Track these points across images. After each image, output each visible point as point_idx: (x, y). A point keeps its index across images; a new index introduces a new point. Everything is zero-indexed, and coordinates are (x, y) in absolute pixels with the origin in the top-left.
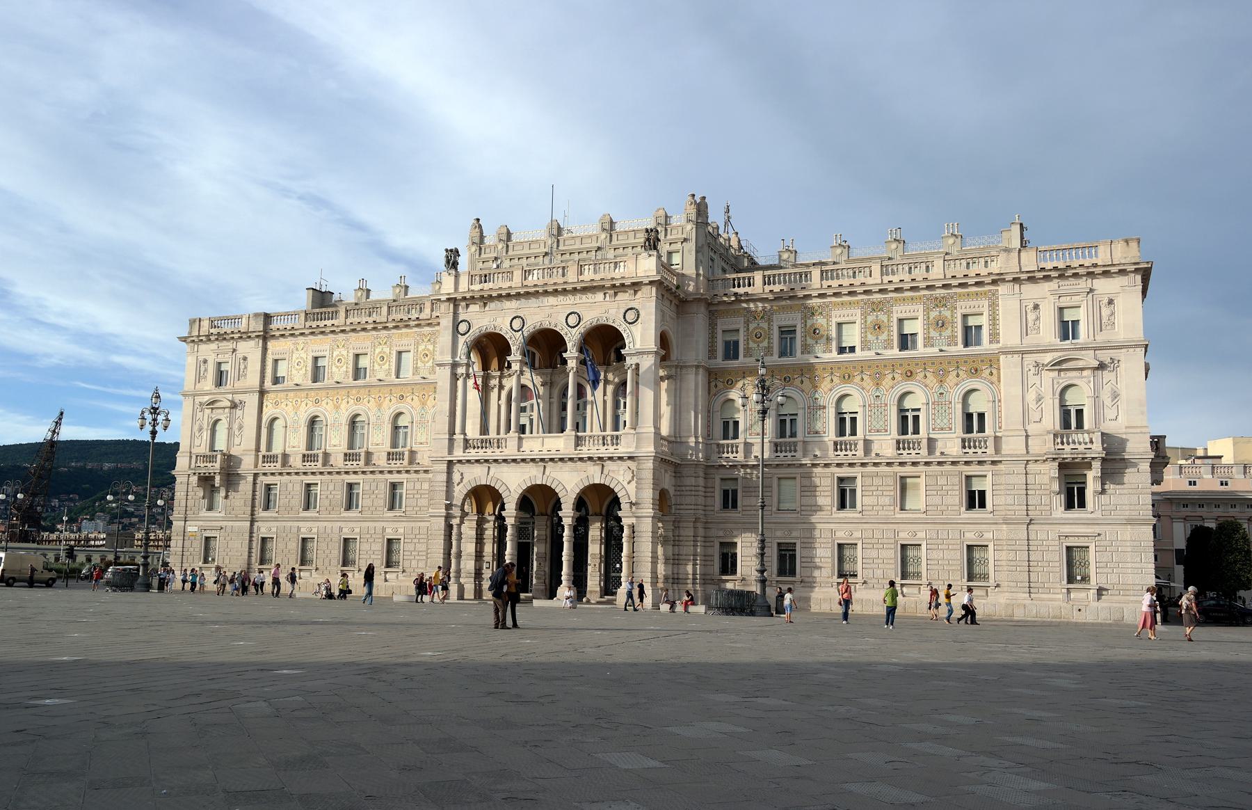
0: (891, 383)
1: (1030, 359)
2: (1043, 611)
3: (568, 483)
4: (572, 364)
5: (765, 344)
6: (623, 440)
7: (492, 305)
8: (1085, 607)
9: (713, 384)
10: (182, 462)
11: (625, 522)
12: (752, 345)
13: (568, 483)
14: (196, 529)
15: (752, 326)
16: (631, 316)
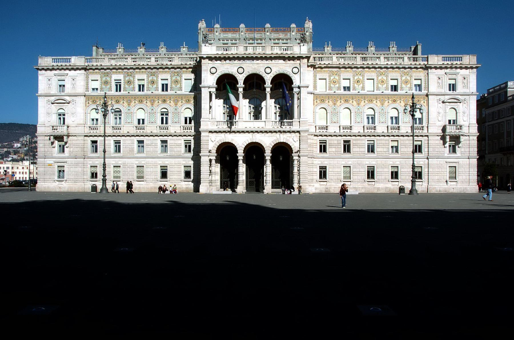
0: (388, 104)
1: (439, 97)
2: (441, 189)
3: (268, 142)
4: (268, 90)
5: (337, 85)
6: (294, 123)
7: (228, 61)
8: (454, 187)
9: (315, 101)
10: (40, 130)
11: (295, 158)
12: (332, 85)
13: (268, 142)
14: (52, 162)
15: (332, 78)
16: (296, 70)
